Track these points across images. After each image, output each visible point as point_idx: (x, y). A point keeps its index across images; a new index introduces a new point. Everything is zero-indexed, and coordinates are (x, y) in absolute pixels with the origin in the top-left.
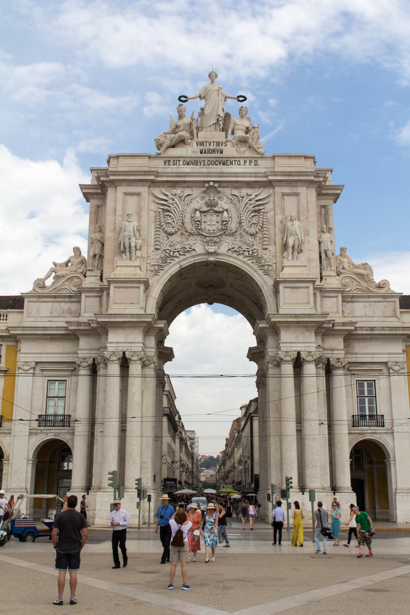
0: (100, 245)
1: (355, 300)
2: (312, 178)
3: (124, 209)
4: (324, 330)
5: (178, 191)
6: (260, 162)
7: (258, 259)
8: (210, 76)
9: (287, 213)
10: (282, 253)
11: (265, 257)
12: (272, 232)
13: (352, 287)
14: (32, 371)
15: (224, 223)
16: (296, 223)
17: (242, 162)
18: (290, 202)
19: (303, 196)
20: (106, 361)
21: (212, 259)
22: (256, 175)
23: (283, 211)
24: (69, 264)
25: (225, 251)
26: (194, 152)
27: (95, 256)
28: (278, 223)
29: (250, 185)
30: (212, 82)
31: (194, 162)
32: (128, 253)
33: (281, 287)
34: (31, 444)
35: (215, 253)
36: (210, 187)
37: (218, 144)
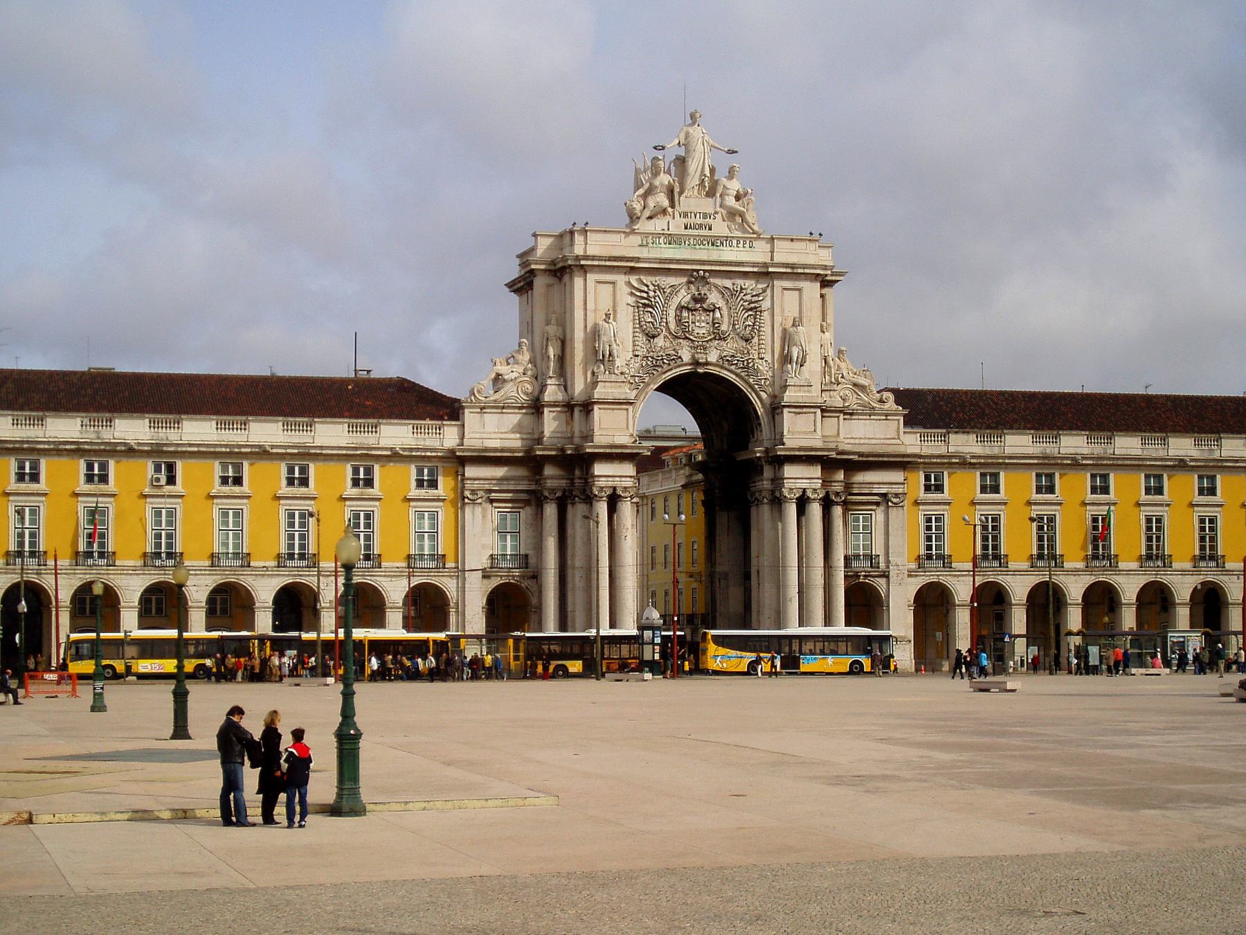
17: (735, 242)
19: (805, 293)
22: (754, 265)
23: (783, 311)
29: (745, 275)
35: (707, 364)
36: (696, 277)
37: (705, 216)
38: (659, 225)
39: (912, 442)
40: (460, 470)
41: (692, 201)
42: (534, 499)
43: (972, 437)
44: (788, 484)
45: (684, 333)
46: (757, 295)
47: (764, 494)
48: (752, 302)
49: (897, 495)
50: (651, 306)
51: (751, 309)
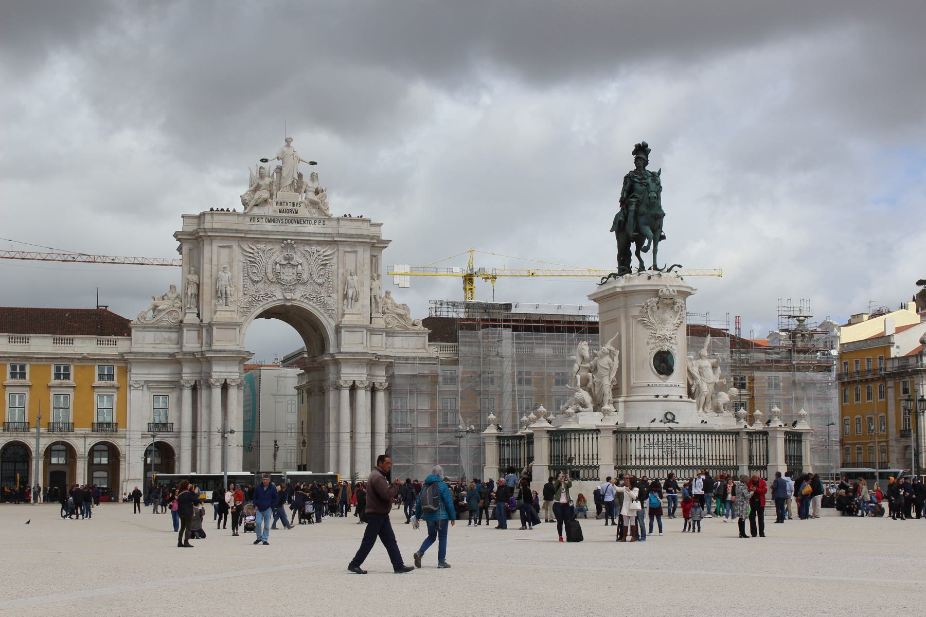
3: (218, 260)
4: (372, 362)
5: (262, 246)
7: (324, 305)
8: (286, 141)
10: (344, 300)
12: (336, 282)
13: (394, 324)
15: (299, 275)
16: (355, 277)
18: (350, 258)
20: (209, 387)
25: (298, 297)
26: (275, 211)
28: (340, 275)
29: (319, 243)
31: (274, 220)
33: (343, 331)
35: (292, 299)
37: (294, 204)
41: (286, 195)
42: (176, 385)
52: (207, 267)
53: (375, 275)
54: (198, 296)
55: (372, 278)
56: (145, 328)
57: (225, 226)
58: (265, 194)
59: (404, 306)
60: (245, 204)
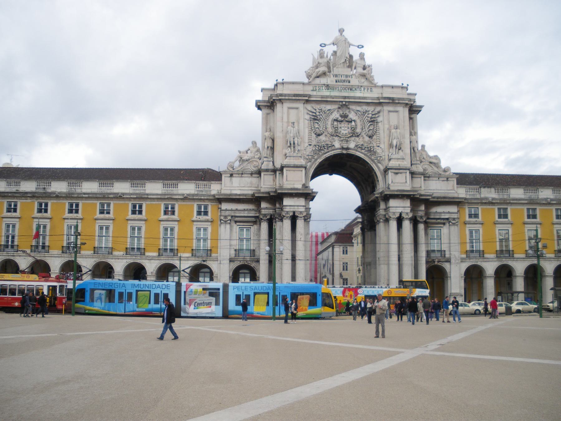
0: (271, 141)
1: (430, 179)
2: (407, 102)
6: (374, 89)
8: (340, 31)
9: (391, 123)
11: (378, 151)
14: (229, 222)
15: (354, 129)
17: (362, 89)
19: (401, 113)
21: (345, 152)
22: (372, 98)
24: (249, 152)
26: (332, 81)
27: (268, 147)
28: (386, 129)
29: (368, 104)
30: (341, 34)
32: (292, 148)
34: (231, 267)
35: (348, 149)
37: (347, 76)
38: (323, 81)
39: (462, 192)
40: (220, 206)
43: (493, 190)
44: (392, 210)
45: (336, 134)
46: (375, 114)
47: (380, 217)
48: (371, 118)
49: (454, 219)
50: (317, 120)
51: (372, 121)
52: (279, 124)
53: (413, 132)
54: (272, 148)
55: (411, 134)
56: (231, 175)
57: (293, 93)
58: (323, 69)
59: (436, 157)
60: (309, 76)
